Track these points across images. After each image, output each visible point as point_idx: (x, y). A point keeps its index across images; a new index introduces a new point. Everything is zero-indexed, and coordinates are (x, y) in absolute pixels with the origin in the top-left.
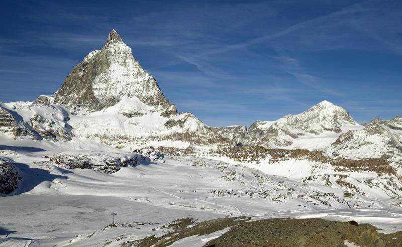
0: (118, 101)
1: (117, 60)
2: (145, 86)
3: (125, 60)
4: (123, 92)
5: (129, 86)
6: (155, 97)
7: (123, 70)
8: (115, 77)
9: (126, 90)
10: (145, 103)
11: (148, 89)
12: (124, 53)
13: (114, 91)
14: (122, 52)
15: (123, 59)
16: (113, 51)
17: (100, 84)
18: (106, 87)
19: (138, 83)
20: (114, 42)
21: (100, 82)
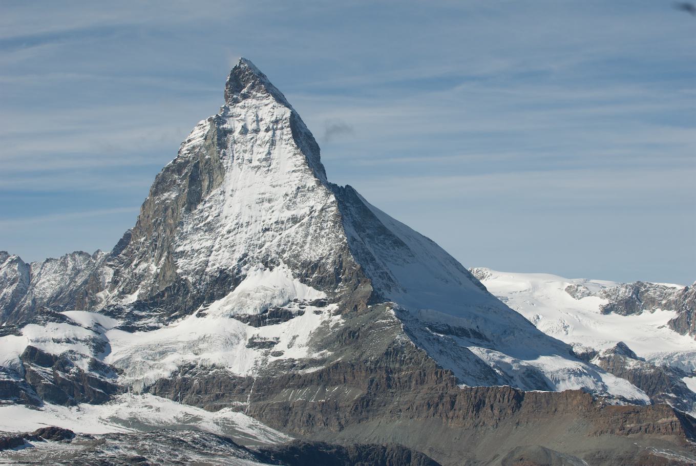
0: (237, 282)
1: (247, 156)
2: (311, 231)
3: (269, 153)
4: (251, 254)
5: (270, 233)
6: (330, 261)
7: (261, 183)
8: (236, 210)
9: (261, 246)
10: (303, 281)
11: (316, 238)
12: (267, 130)
13: (227, 255)
14: (263, 127)
15: (265, 149)
16: (238, 127)
17: (196, 237)
18: (209, 243)
19: (295, 220)
20: (245, 97)
21: (196, 230)
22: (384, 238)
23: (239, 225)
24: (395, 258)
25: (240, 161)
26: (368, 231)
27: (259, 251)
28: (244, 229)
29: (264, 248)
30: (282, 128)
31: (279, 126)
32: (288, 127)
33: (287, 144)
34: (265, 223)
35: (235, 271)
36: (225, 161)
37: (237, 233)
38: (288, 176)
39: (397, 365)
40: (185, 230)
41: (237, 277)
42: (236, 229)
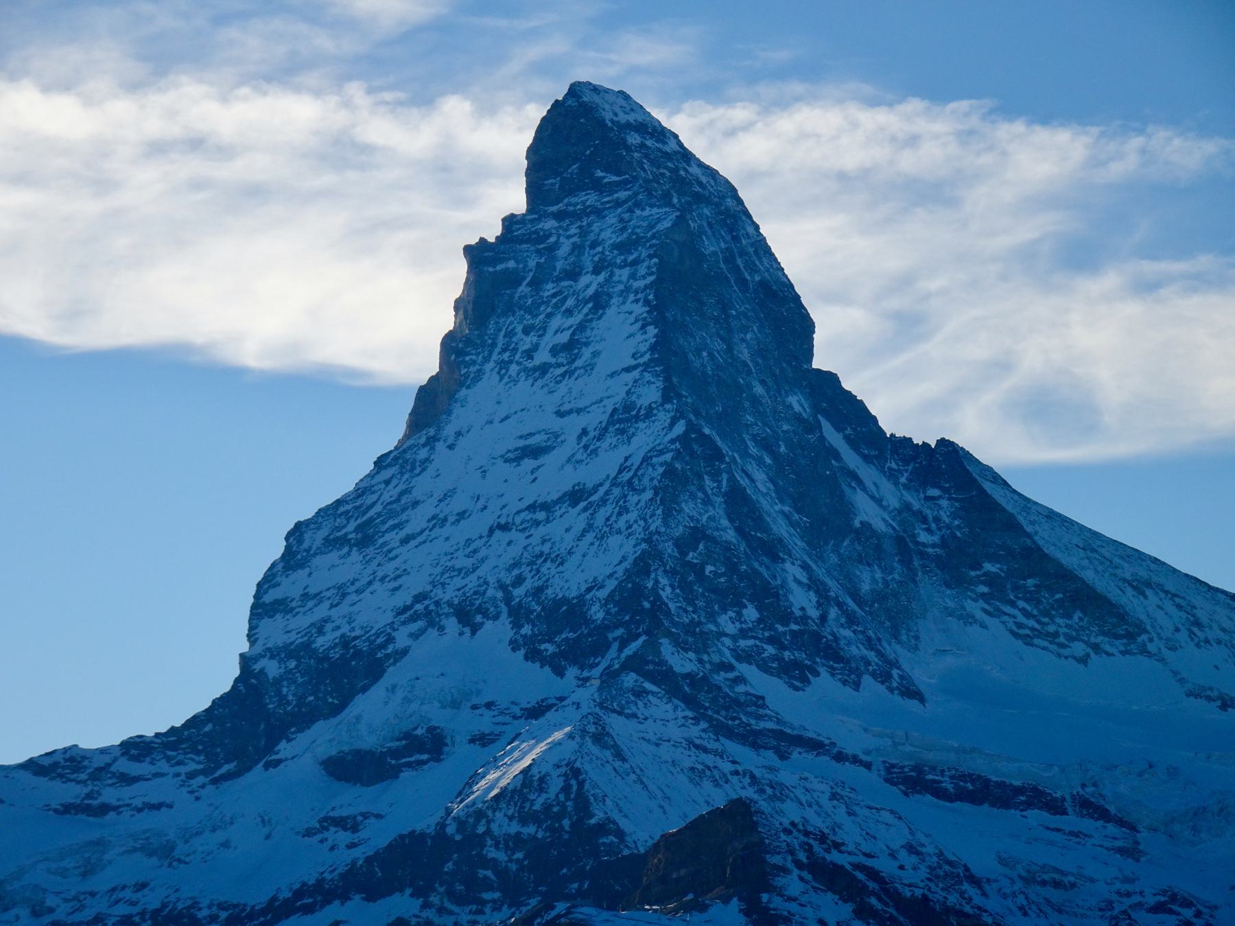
1: (527, 342)
3: (581, 327)
6: (603, 594)
14: (588, 261)
20: (571, 189)
22: (1035, 586)
23: (438, 521)
24: (1062, 639)
25: (506, 356)
26: (988, 567)
27: (458, 582)
28: (448, 530)
29: (473, 577)
30: (635, 263)
31: (631, 258)
32: (650, 257)
33: (637, 301)
34: (505, 511)
35: (379, 641)
36: (467, 358)
37: (425, 542)
38: (610, 382)
40: (305, 545)
41: (379, 655)
42: (427, 532)
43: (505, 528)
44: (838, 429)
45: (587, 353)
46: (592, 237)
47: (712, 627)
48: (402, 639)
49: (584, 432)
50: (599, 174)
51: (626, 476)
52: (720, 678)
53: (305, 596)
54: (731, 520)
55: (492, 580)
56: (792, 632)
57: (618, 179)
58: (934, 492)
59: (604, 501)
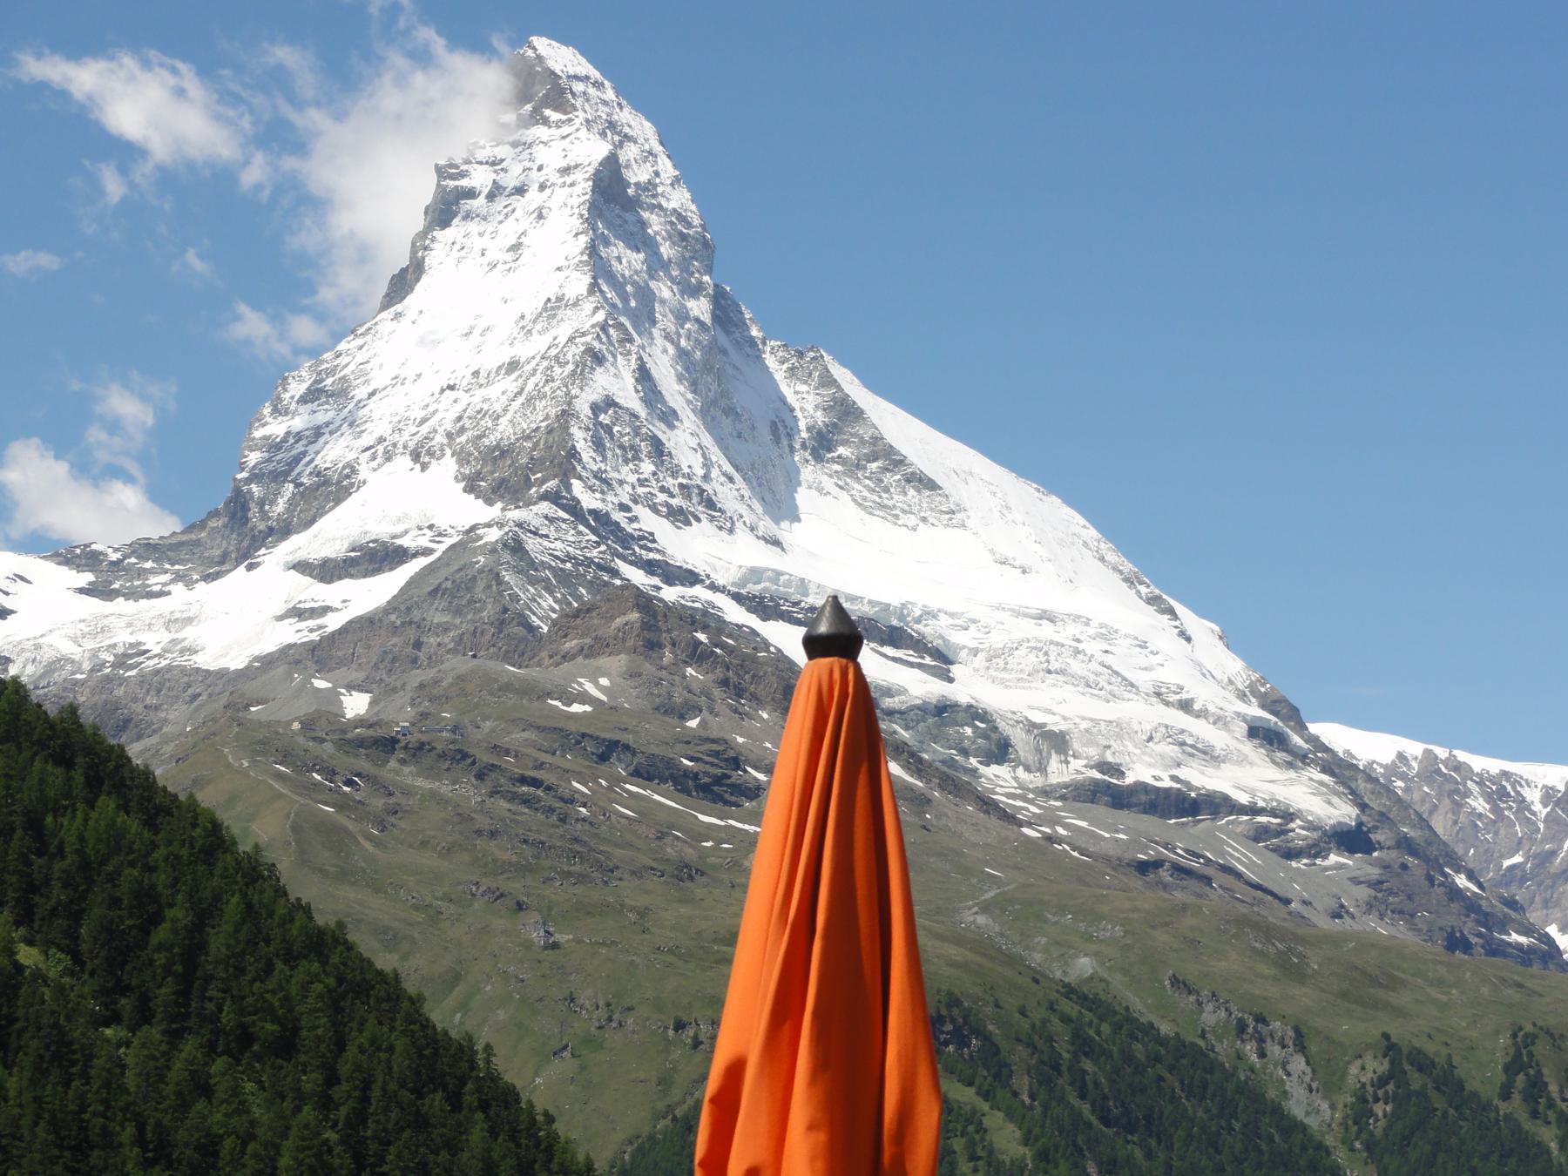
9: (423, 421)
10: (471, 488)
25: (463, 253)
26: (841, 450)
27: (414, 429)
30: (572, 185)
31: (569, 180)
39: (446, 618)
43: (451, 388)
44: (728, 333)
45: (526, 252)
46: (538, 162)
47: (616, 475)
48: (364, 472)
49: (523, 317)
50: (548, 112)
51: (553, 352)
52: (618, 516)
53: (288, 433)
54: (637, 391)
55: (441, 430)
56: (682, 486)
57: (564, 118)
58: (804, 388)
59: (535, 370)
